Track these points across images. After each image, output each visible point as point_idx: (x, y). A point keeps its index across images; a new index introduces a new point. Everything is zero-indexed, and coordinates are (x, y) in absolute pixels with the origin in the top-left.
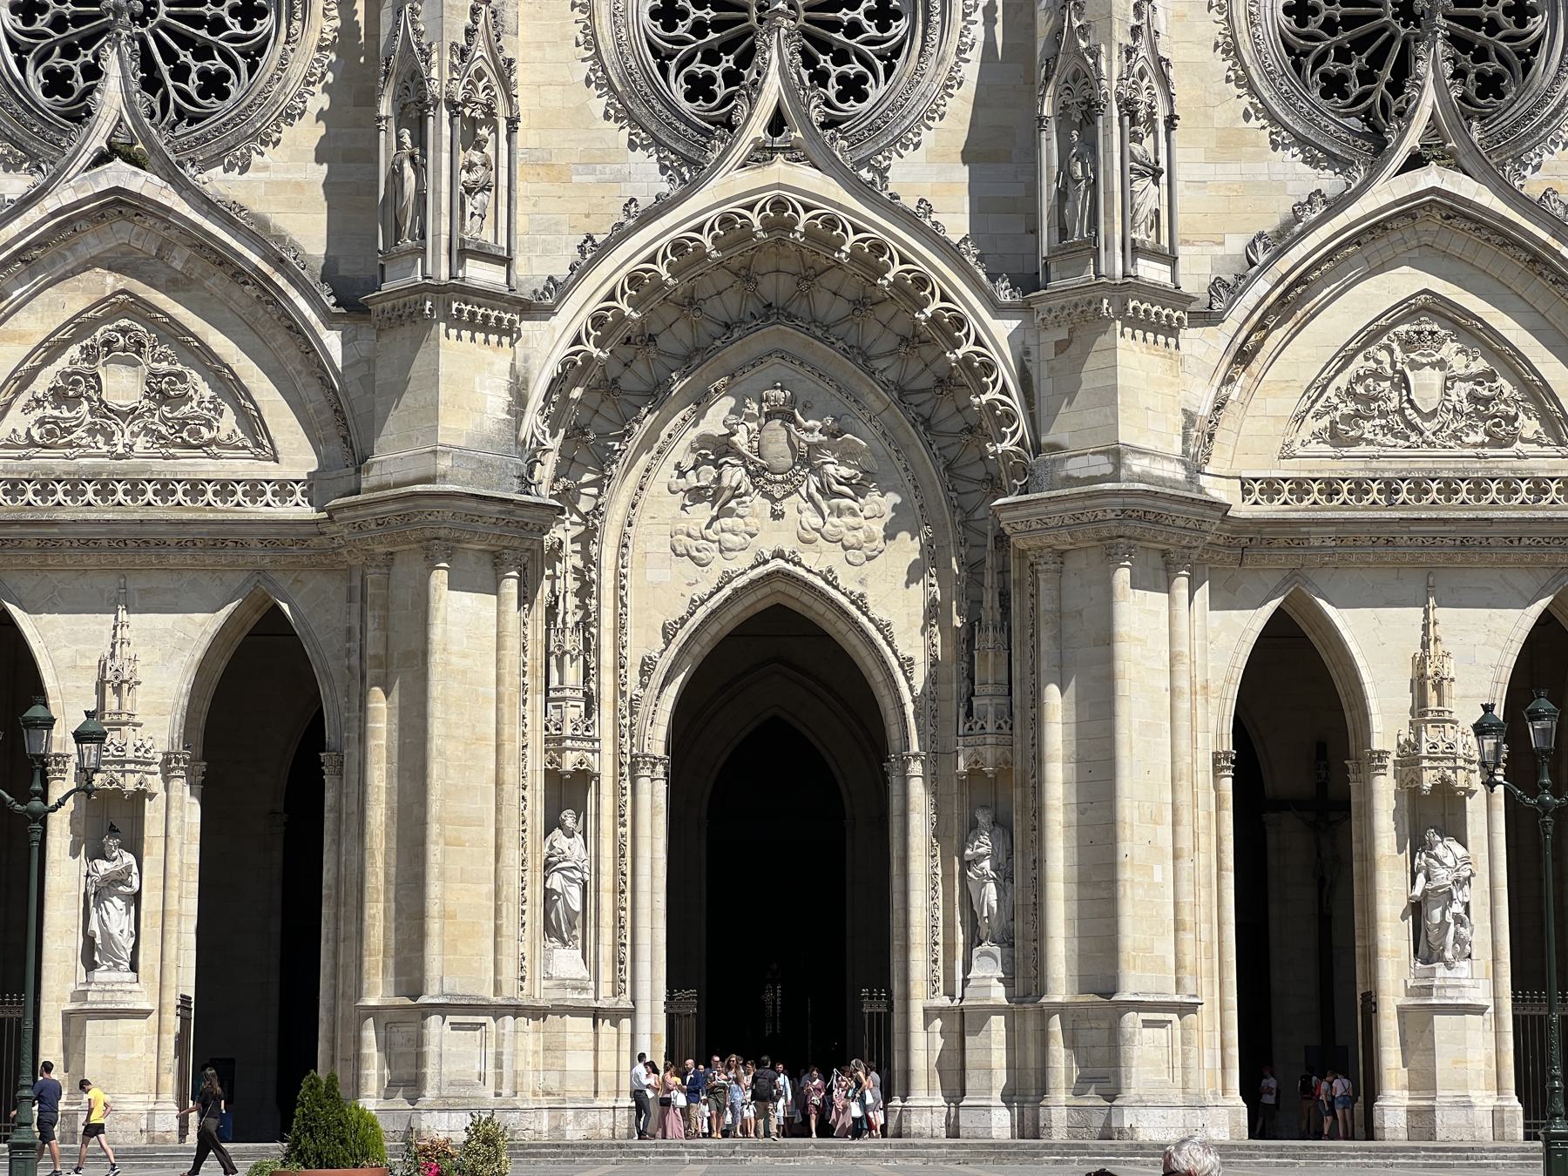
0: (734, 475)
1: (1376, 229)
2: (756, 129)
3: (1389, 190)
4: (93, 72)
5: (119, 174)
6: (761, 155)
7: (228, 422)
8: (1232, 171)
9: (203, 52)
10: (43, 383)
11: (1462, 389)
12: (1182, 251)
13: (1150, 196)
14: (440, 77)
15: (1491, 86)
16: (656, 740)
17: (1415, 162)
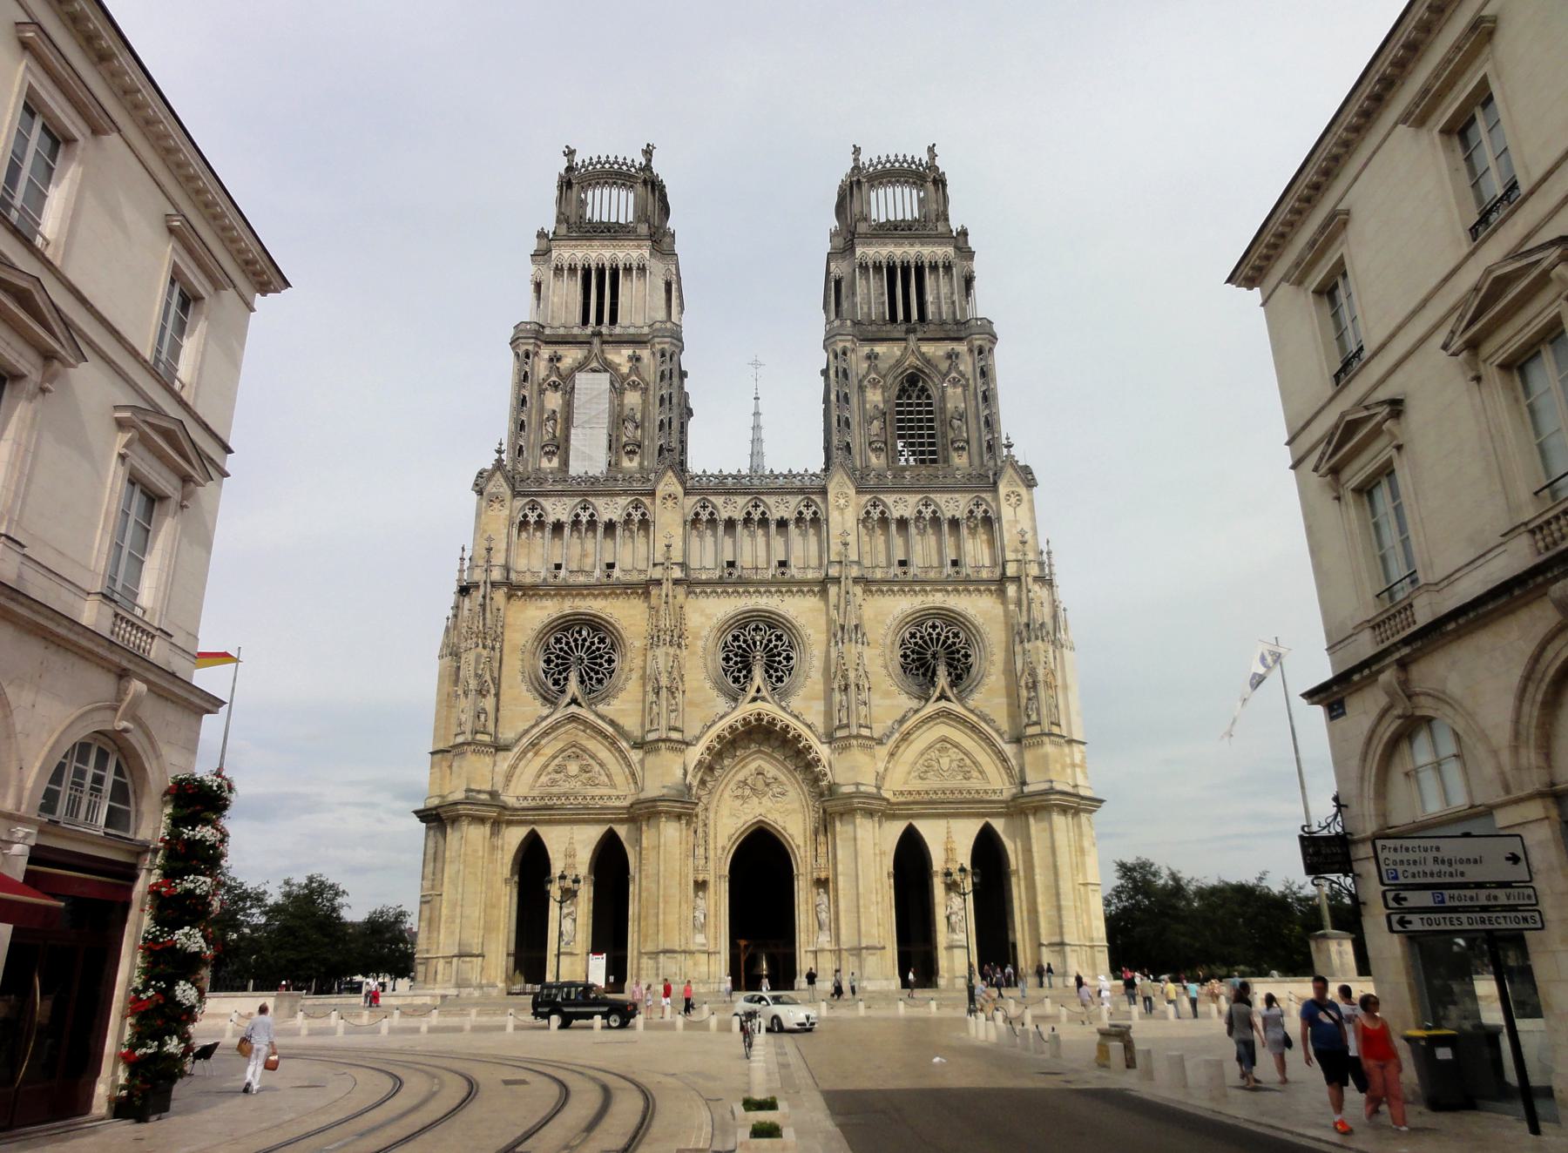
0: (748, 792)
1: (930, 718)
2: (752, 693)
3: (931, 708)
4: (566, 679)
5: (574, 708)
8: (888, 702)
9: (597, 673)
10: (550, 769)
11: (954, 765)
12: (874, 726)
13: (863, 710)
14: (664, 681)
15: (959, 677)
16: (725, 870)
17: (938, 699)
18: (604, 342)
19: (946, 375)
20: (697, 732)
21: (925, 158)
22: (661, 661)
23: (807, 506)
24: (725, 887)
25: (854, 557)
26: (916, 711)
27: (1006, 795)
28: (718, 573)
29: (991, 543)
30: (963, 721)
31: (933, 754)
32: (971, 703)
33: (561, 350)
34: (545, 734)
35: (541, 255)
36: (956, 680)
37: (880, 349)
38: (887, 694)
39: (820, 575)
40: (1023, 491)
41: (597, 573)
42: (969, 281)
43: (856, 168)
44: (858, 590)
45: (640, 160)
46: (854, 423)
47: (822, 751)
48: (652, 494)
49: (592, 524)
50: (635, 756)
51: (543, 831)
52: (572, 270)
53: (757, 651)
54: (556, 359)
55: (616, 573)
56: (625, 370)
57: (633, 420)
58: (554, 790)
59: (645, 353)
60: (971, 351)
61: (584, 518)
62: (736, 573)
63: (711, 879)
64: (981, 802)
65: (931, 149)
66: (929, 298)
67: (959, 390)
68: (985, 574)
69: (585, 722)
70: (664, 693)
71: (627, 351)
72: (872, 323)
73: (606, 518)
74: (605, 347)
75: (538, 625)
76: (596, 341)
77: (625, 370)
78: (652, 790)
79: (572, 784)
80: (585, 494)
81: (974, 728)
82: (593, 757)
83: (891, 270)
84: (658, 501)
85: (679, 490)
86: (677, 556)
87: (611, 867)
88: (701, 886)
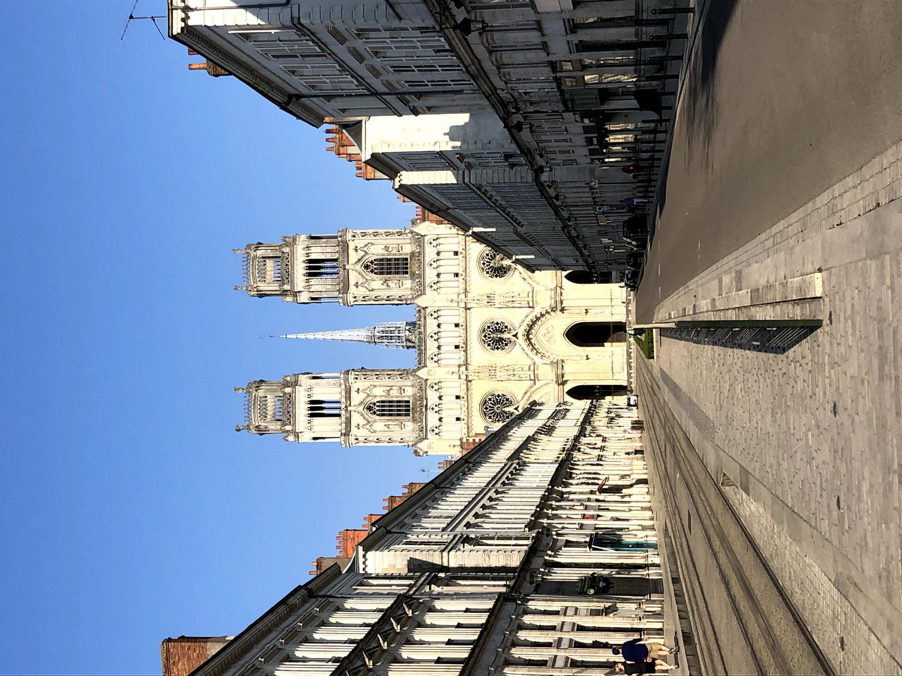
13: (522, 295)
19: (366, 253)
33: (353, 424)
37: (352, 281)
39: (462, 312)
47: (537, 311)
57: (388, 391)
59: (354, 388)
71: (354, 394)
77: (362, 396)
80: (426, 409)
83: (310, 275)
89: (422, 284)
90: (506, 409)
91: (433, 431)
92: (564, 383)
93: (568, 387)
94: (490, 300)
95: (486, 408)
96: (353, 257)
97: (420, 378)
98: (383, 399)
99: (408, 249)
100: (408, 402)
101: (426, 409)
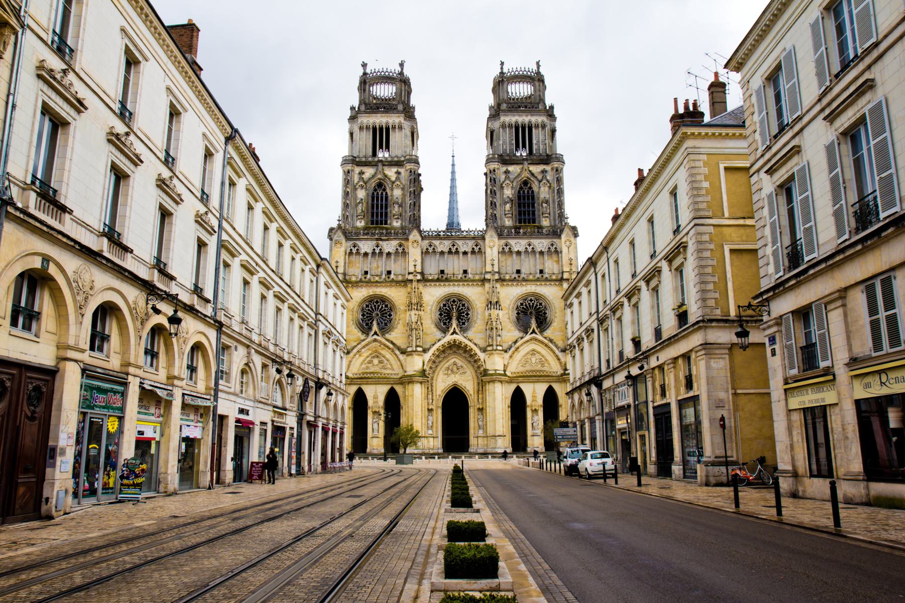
2: (452, 331)
5: (375, 337)
6: (452, 334)
7: (389, 366)
13: (499, 338)
15: (541, 323)
18: (384, 165)
19: (540, 182)
20: (428, 346)
21: (535, 68)
22: (413, 317)
23: (476, 245)
24: (440, 411)
25: (497, 270)
26: (522, 338)
27: (559, 373)
28: (436, 277)
29: (558, 262)
30: (543, 343)
31: (529, 356)
32: (546, 334)
33: (365, 169)
34: (364, 347)
35: (352, 119)
36: (538, 326)
37: (511, 168)
38: (509, 331)
40: (572, 239)
41: (384, 276)
42: (553, 131)
43: (502, 73)
44: (498, 285)
45: (398, 69)
46: (498, 204)
47: (482, 356)
48: (407, 239)
49: (381, 253)
50: (402, 357)
51: (364, 387)
52: (368, 128)
53: (454, 313)
54: (361, 173)
55: (392, 276)
56: (393, 179)
58: (368, 371)
59: (402, 170)
60: (552, 169)
61: (377, 251)
62: (445, 277)
63: (434, 407)
64: (548, 376)
65: (538, 63)
66: (534, 142)
67: (547, 189)
68: (554, 277)
69: (380, 342)
70: (414, 331)
71: (394, 170)
72: (508, 155)
73: (387, 251)
74: (386, 168)
75: (359, 300)
76: (380, 164)
77: (393, 179)
78: (410, 372)
79: (375, 367)
81: (546, 345)
82: (384, 357)
84: (410, 244)
85: (419, 239)
86: (419, 269)
87: (393, 403)
88: (430, 410)
89: (509, 236)
90: (375, 323)
91: (354, 246)
92: (401, 383)
93: (399, 389)
94: (493, 304)
95: (377, 302)
96: (536, 169)
97: (410, 232)
98: (390, 198)
99: (545, 223)
100: (386, 224)
101: (377, 239)
